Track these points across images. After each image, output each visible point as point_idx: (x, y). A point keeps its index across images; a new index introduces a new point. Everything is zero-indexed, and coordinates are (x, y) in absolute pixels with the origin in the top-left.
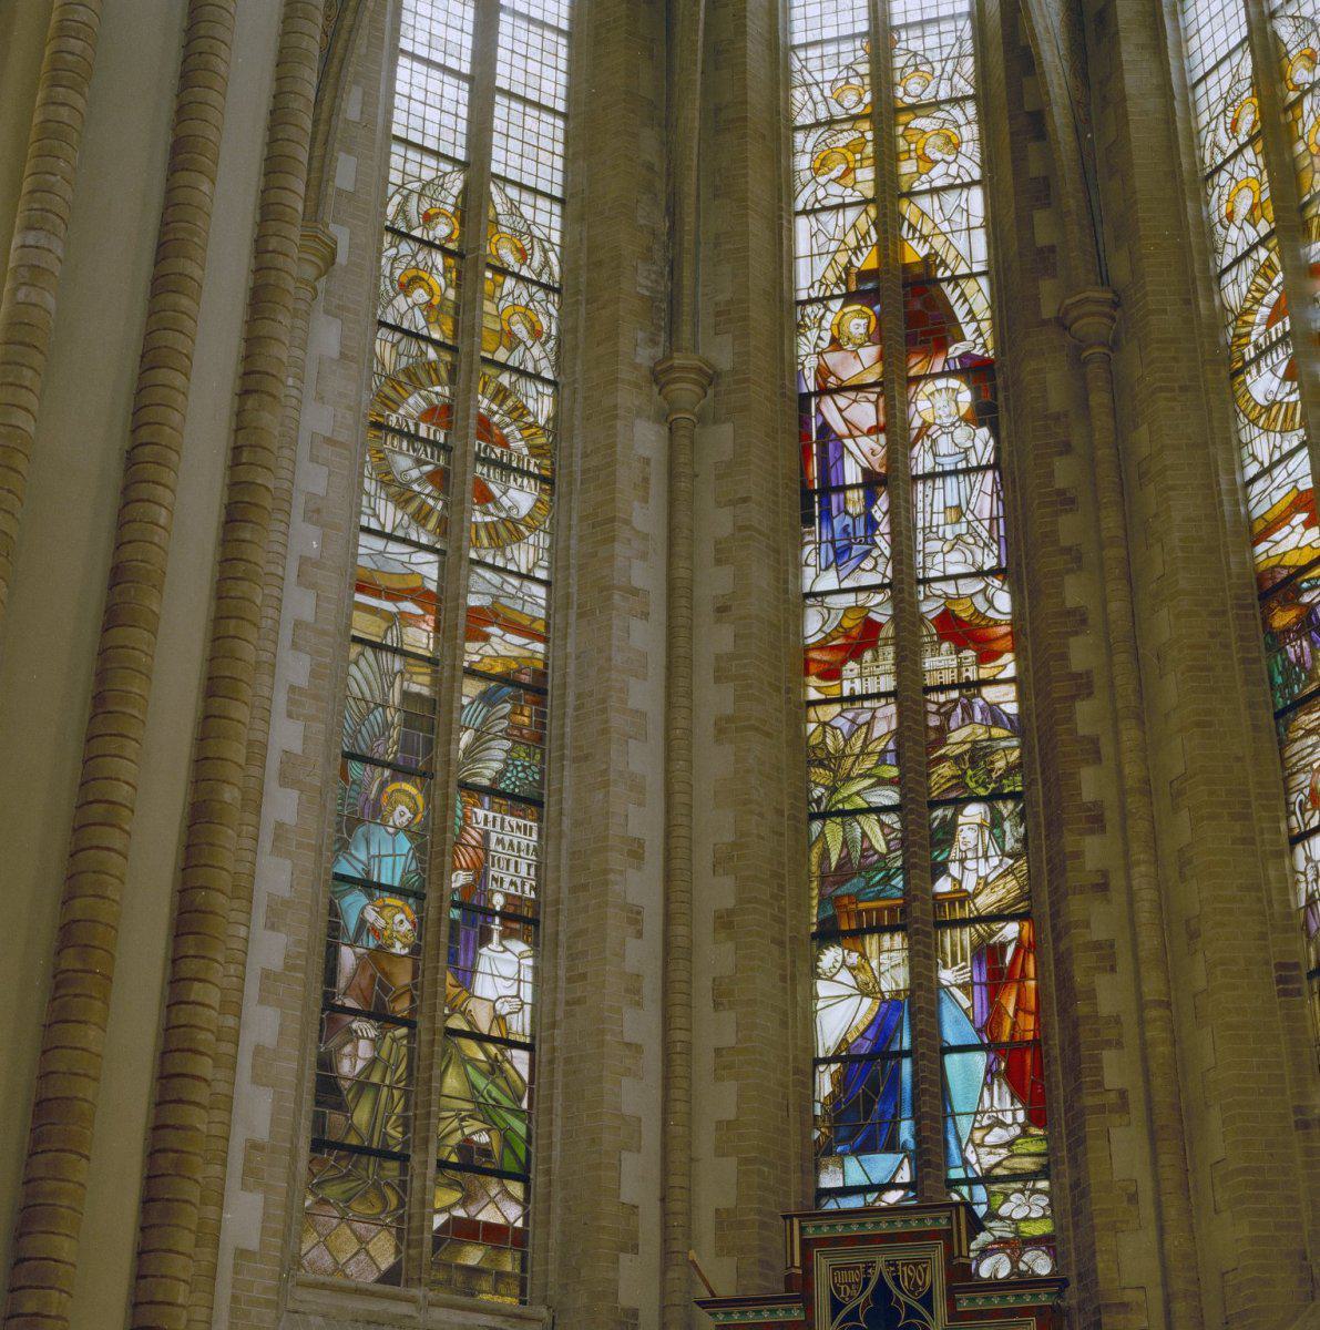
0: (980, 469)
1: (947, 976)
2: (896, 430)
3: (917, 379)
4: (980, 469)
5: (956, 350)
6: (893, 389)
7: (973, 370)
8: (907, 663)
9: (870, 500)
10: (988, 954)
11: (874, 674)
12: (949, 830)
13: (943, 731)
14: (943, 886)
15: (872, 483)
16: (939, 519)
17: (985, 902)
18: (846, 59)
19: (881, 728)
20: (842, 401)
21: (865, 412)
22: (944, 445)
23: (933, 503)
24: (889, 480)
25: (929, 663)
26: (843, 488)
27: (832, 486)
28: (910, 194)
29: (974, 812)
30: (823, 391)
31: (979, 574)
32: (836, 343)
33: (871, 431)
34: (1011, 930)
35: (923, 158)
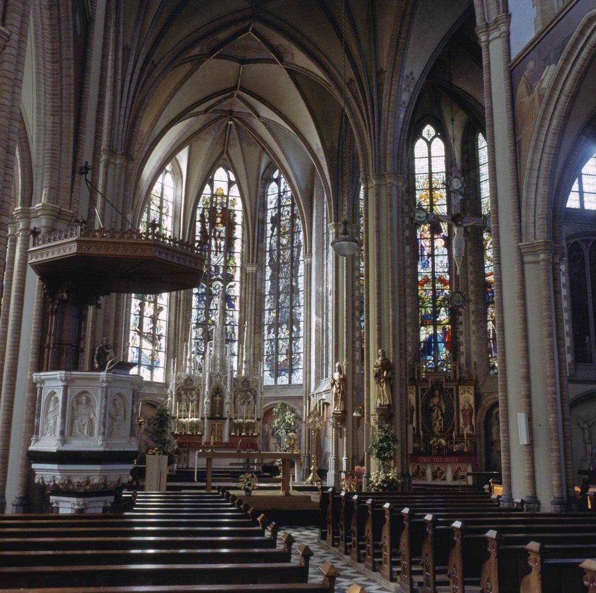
0: (445, 255)
1: (438, 332)
2: (432, 247)
3: (436, 238)
4: (445, 255)
5: (442, 234)
6: (432, 240)
7: (444, 238)
8: (434, 286)
9: (428, 258)
10: (444, 329)
11: (428, 287)
12: (439, 311)
13: (438, 296)
14: (438, 319)
15: (429, 256)
16: (439, 263)
17: (444, 322)
18: (425, 178)
19: (430, 295)
20: (424, 241)
21: (428, 244)
22: (440, 250)
23: (437, 260)
24: (432, 255)
25: (437, 285)
26: (424, 256)
27: (423, 255)
28: (435, 205)
29: (443, 309)
30: (421, 239)
31: (444, 272)
32: (423, 231)
33: (429, 247)
34: (447, 326)
35: (437, 199)
